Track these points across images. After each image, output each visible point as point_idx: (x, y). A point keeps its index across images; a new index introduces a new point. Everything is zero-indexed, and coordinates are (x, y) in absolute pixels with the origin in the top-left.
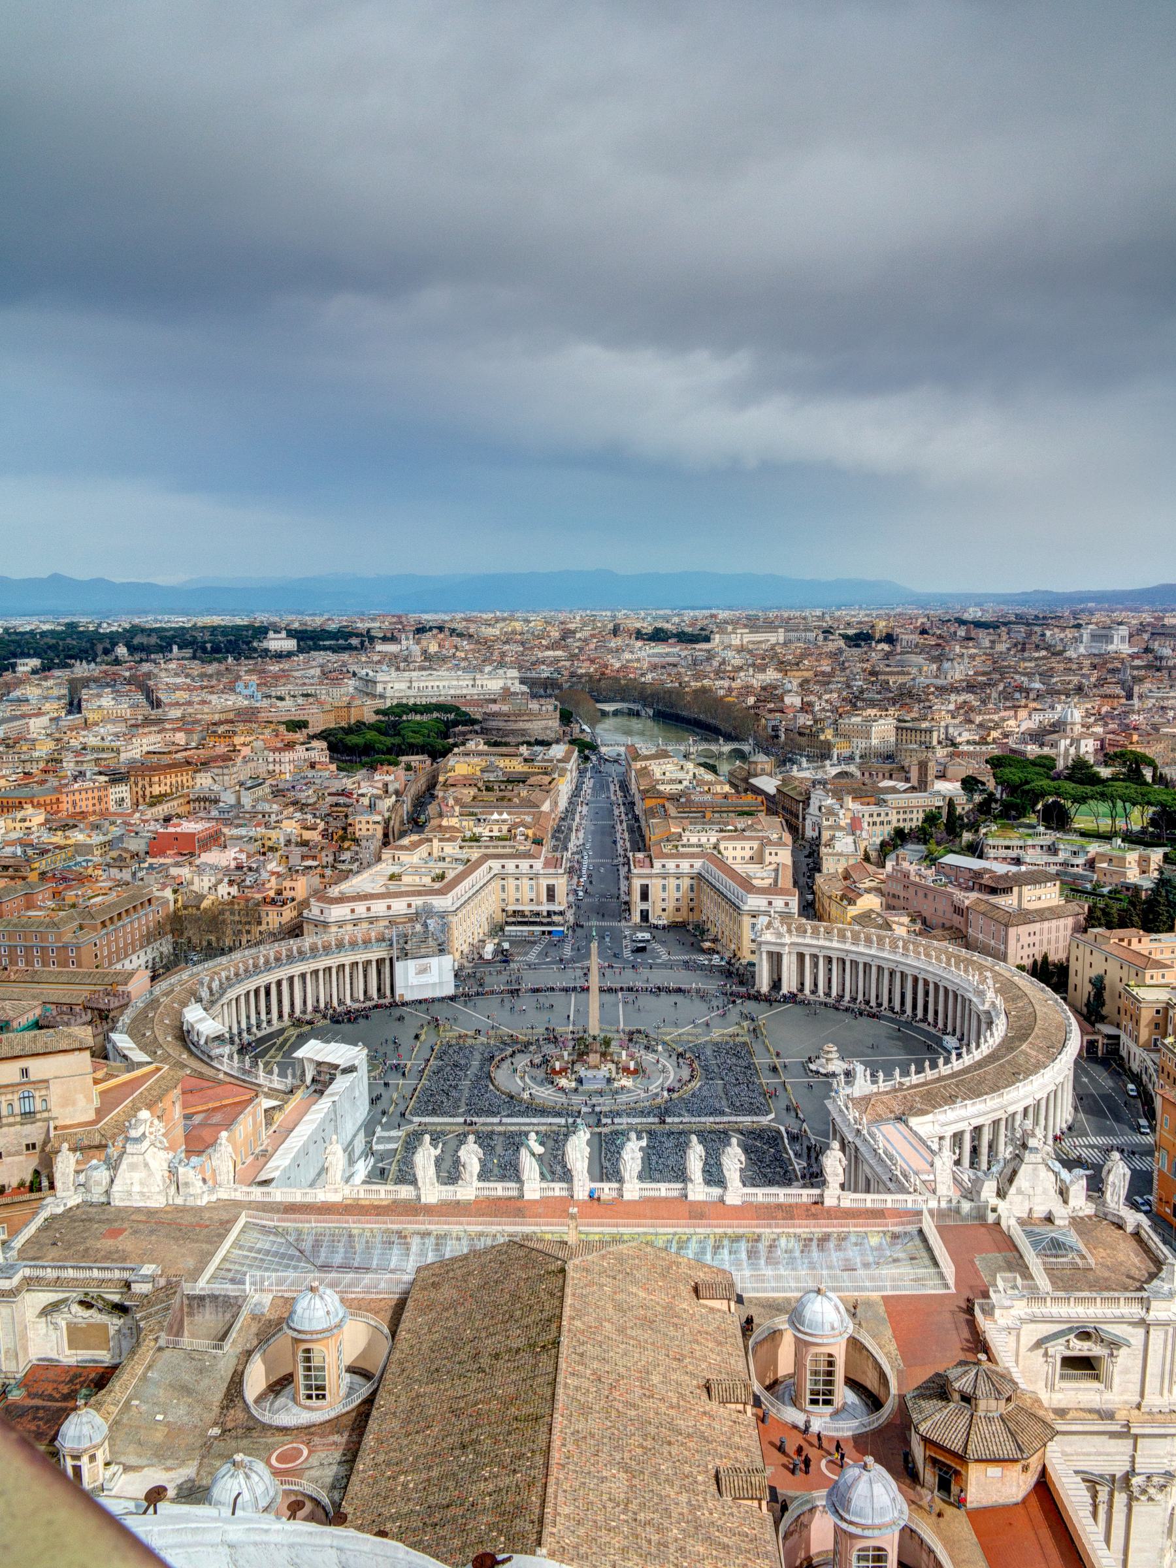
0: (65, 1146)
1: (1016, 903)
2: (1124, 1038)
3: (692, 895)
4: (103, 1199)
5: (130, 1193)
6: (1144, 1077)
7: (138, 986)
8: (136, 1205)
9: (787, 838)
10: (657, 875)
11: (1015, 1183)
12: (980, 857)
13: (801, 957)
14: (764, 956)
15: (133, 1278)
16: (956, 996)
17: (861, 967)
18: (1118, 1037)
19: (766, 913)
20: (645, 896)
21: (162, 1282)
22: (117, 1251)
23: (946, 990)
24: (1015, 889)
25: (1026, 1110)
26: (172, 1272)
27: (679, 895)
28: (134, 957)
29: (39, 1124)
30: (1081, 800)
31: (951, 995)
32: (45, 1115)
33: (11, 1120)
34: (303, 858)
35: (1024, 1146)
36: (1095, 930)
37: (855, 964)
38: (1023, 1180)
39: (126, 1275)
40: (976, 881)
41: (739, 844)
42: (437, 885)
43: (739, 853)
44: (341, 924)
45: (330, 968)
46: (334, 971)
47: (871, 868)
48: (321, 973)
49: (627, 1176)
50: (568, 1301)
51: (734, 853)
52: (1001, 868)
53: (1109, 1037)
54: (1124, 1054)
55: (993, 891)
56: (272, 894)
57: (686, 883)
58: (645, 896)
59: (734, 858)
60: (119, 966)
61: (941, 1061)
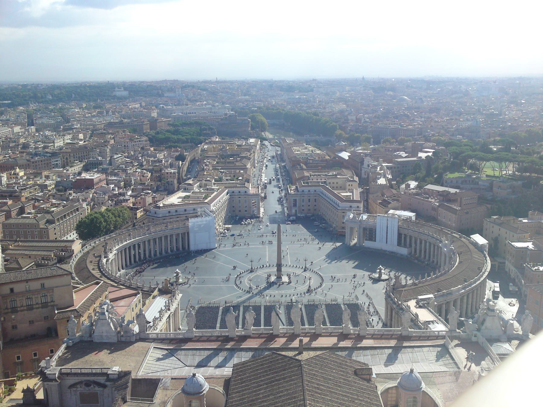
0: (73, 316)
1: (459, 205)
2: (507, 262)
3: (315, 203)
4: (89, 339)
5: (102, 336)
6: (517, 280)
7: (77, 247)
8: (104, 341)
9: (356, 179)
11: (485, 324)
12: (442, 185)
15: (109, 372)
16: (434, 246)
18: (505, 263)
20: (295, 205)
21: (123, 374)
22: (100, 362)
23: (430, 244)
24: (459, 199)
25: (468, 294)
26: (125, 369)
27: (309, 204)
28: (71, 234)
29: (50, 308)
30: (488, 160)
31: (432, 246)
32: (52, 304)
33: (37, 306)
34: (143, 190)
35: (488, 309)
36: (495, 217)
38: (489, 323)
39: (105, 371)
41: (335, 181)
42: (206, 201)
43: (335, 185)
45: (161, 237)
46: (163, 239)
47: (394, 191)
49: (317, 323)
50: (305, 378)
51: (334, 185)
52: (453, 191)
53: (501, 263)
54: (507, 270)
55: (449, 201)
56: (131, 205)
58: (295, 205)
59: (333, 187)
60: (65, 238)
61: (432, 274)
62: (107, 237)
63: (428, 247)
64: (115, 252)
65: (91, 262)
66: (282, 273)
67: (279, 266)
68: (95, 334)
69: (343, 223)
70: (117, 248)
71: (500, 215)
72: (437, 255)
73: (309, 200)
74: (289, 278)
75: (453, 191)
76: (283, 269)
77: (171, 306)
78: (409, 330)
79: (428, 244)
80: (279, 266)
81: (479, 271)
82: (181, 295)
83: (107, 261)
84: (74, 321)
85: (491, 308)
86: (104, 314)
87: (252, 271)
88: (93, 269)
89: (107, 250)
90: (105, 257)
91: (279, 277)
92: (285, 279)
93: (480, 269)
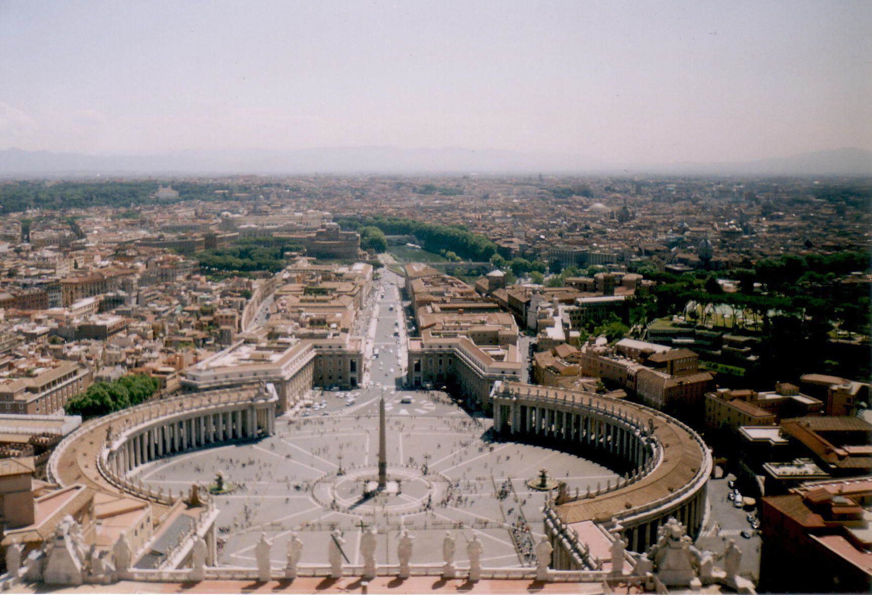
9: (516, 329)
10: (427, 355)
13: (524, 409)
14: (499, 408)
17: (565, 415)
19: (500, 378)
36: (722, 391)
37: (560, 414)
40: (644, 357)
44: (207, 389)
47: (573, 349)
48: (193, 422)
57: (445, 360)
62: (114, 416)
63: (618, 437)
64: (123, 439)
65: (85, 455)
66: (387, 477)
67: (382, 466)
68: (50, 569)
69: (492, 398)
70: (129, 432)
71: (732, 389)
72: (633, 450)
73: (441, 361)
74: (400, 486)
75: (659, 349)
76: (389, 471)
77: (198, 527)
78: (550, 571)
79: (619, 432)
80: (382, 466)
81: (692, 474)
82: (217, 512)
83: (111, 454)
84: (16, 550)
85: (675, 536)
86: (61, 538)
87: (340, 474)
88: (86, 467)
89: (111, 437)
90: (108, 447)
91: (382, 485)
92: (391, 487)
93: (696, 471)
